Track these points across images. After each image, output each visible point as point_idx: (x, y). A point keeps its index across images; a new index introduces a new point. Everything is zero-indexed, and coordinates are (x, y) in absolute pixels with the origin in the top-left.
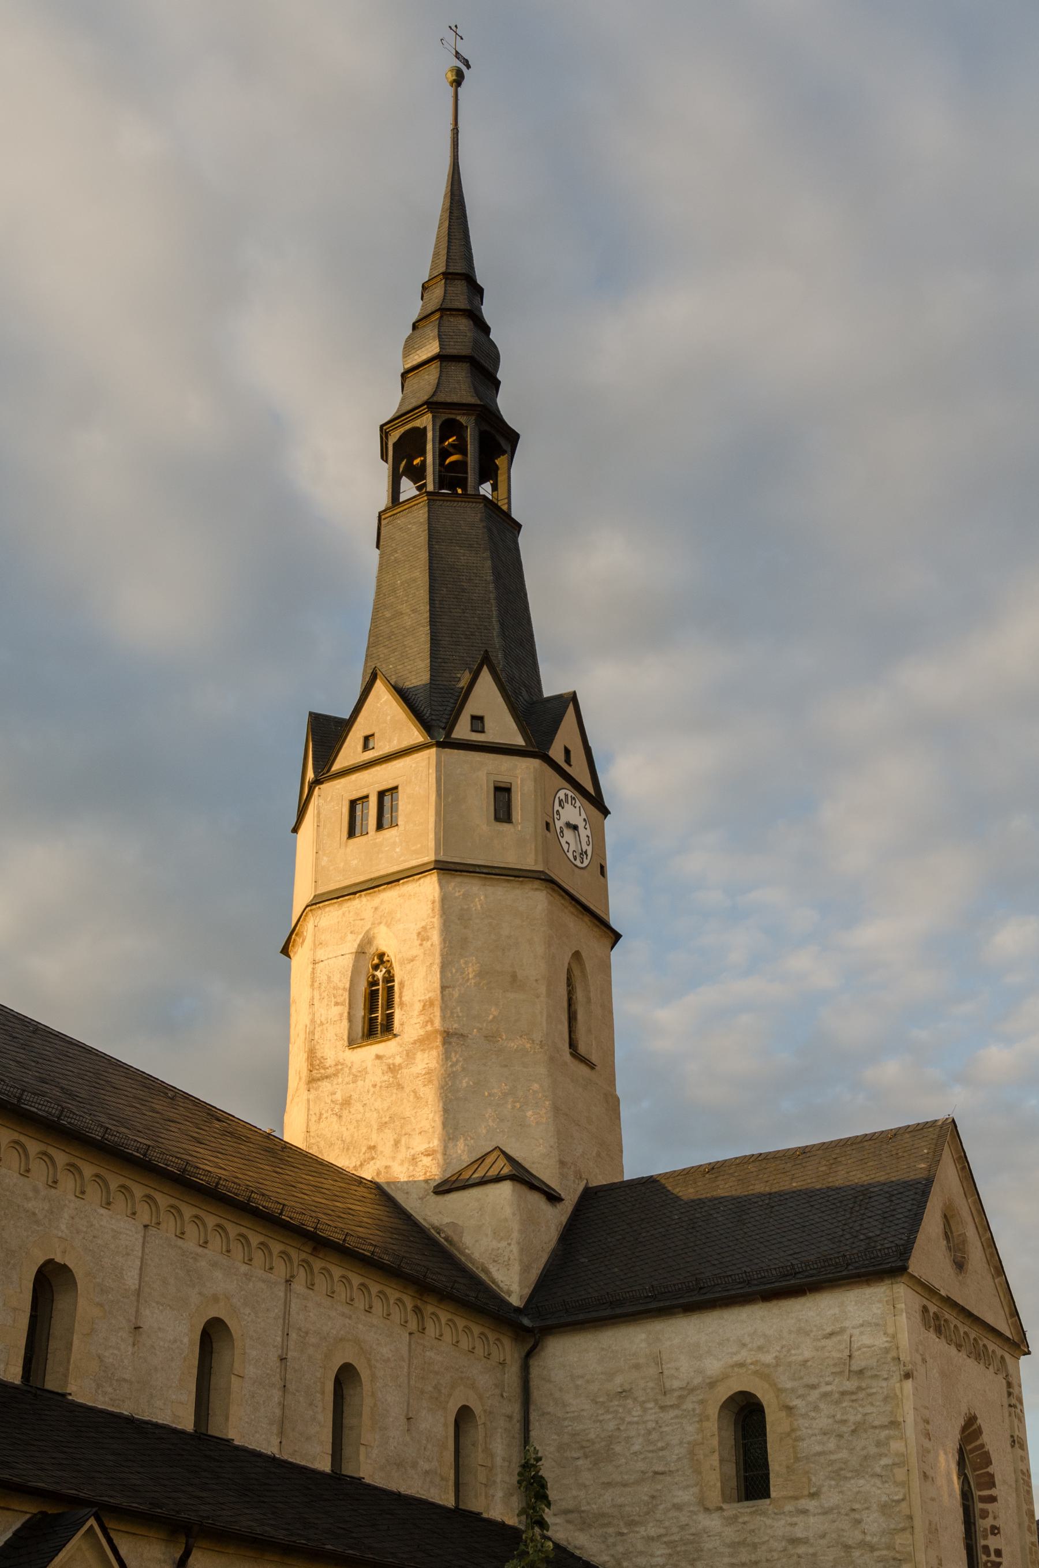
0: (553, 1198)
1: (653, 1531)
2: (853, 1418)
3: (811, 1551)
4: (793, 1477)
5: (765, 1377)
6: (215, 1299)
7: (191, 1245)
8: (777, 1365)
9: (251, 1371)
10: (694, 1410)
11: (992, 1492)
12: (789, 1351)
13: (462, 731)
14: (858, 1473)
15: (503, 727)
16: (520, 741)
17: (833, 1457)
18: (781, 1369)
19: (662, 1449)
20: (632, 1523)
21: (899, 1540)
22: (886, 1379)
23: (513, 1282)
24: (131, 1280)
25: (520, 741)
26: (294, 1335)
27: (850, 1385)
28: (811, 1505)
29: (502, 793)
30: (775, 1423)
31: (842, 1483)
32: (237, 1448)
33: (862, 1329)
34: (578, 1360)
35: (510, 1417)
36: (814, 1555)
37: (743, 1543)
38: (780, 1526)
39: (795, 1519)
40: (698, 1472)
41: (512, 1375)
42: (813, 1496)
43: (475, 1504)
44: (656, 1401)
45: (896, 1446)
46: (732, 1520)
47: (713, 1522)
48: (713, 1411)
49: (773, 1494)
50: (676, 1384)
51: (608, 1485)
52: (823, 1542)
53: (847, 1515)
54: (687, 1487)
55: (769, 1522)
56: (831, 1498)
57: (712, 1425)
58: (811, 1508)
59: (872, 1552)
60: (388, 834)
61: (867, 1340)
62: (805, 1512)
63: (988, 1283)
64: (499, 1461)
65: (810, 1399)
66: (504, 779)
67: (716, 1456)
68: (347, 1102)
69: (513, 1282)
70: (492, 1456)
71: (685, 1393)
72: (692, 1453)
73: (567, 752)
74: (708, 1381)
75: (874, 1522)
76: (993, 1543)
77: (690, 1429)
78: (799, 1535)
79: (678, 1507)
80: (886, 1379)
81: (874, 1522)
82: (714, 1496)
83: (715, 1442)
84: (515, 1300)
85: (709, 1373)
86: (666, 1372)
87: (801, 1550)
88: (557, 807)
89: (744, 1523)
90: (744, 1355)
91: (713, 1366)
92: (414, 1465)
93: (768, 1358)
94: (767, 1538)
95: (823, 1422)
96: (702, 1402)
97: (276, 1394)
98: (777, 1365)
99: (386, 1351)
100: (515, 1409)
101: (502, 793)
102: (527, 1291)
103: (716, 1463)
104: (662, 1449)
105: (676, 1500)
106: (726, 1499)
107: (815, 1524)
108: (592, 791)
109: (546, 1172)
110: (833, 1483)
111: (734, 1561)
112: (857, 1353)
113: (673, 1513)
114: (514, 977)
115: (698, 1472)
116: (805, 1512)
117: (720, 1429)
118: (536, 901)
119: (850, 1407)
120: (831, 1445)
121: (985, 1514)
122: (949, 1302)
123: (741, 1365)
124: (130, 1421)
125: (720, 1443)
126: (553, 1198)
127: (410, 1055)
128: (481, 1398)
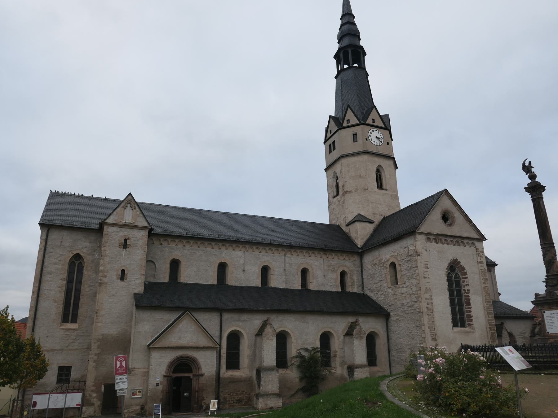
0: (372, 222)
1: (381, 293)
2: (410, 266)
5: (396, 258)
6: (265, 262)
7: (258, 253)
9: (276, 273)
11: (466, 276)
13: (345, 124)
14: (412, 278)
15: (354, 120)
16: (358, 122)
20: (378, 291)
21: (419, 292)
23: (360, 243)
24: (242, 262)
25: (358, 122)
26: (288, 265)
28: (404, 285)
29: (355, 135)
30: (398, 268)
32: (274, 288)
34: (368, 259)
35: (358, 271)
37: (394, 294)
38: (399, 291)
41: (358, 262)
42: (405, 283)
43: (349, 289)
45: (417, 271)
46: (392, 290)
47: (390, 290)
48: (388, 266)
50: (383, 261)
51: (374, 283)
56: (407, 284)
57: (388, 269)
60: (335, 151)
61: (411, 248)
62: (403, 287)
63: (467, 225)
64: (355, 280)
66: (354, 132)
68: (333, 209)
69: (360, 243)
70: (353, 280)
73: (373, 120)
75: (414, 289)
76: (466, 288)
79: (384, 287)
81: (414, 289)
82: (390, 286)
84: (359, 246)
87: (404, 295)
88: (369, 134)
90: (393, 254)
91: (388, 257)
92: (327, 284)
93: (396, 254)
95: (405, 267)
97: (284, 277)
99: (316, 264)
100: (360, 269)
101: (355, 135)
102: (362, 244)
106: (392, 285)
107: (404, 290)
108: (383, 126)
109: (371, 218)
114: (360, 176)
116: (403, 287)
118: (365, 157)
120: (407, 272)
121: (464, 282)
122: (438, 235)
123: (392, 256)
124: (241, 288)
126: (372, 222)
127: (341, 198)
128: (348, 268)
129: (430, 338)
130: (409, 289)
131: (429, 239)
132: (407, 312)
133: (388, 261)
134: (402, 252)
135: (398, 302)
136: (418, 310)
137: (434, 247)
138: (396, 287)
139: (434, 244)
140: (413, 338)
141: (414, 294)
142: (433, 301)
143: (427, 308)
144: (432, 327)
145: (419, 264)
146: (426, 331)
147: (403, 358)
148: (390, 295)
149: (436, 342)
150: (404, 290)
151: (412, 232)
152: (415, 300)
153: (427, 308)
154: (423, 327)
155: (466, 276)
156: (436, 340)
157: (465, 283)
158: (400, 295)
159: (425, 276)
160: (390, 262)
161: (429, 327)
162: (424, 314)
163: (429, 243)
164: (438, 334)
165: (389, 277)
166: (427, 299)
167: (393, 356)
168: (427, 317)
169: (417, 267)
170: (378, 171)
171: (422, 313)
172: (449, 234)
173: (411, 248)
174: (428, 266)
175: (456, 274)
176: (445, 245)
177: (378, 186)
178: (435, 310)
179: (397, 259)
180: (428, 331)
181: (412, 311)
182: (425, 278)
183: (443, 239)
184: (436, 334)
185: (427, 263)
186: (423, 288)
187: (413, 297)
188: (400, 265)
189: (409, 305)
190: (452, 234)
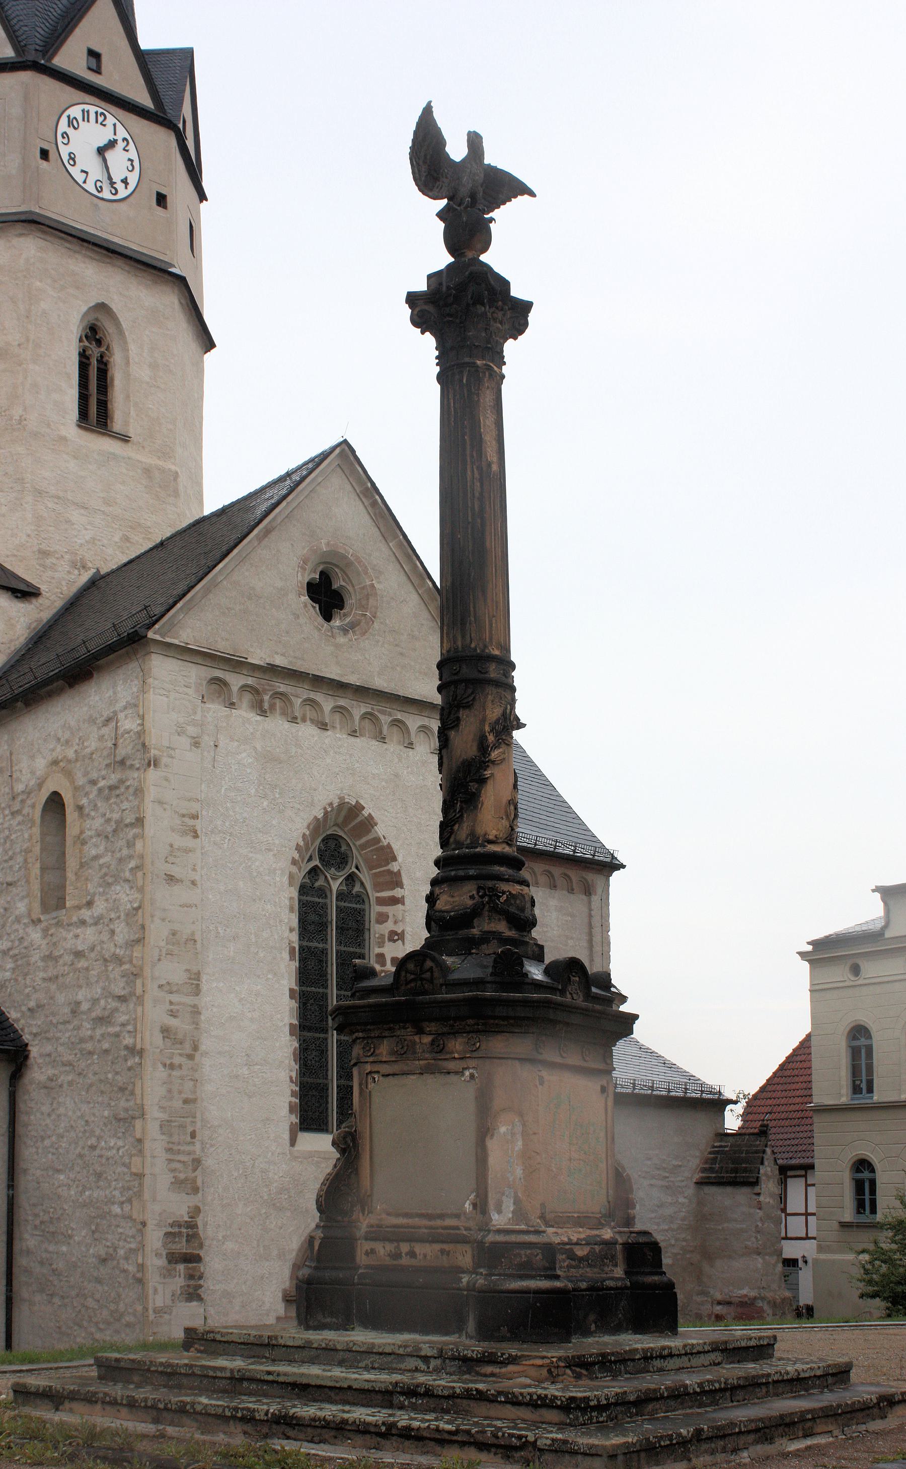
3: (86, 964)
4: (79, 885)
5: (69, 774)
8: (77, 760)
10: (28, 814)
12: (83, 743)
17: (102, 861)
18: (78, 764)
19: (11, 858)
22: (138, 769)
27: (114, 778)
28: (86, 914)
31: (107, 890)
33: (126, 712)
36: (87, 969)
39: (79, 931)
40: (28, 882)
44: (9, 806)
49: (68, 904)
50: (20, 787)
52: (93, 955)
53: (107, 925)
54: (23, 898)
55: (64, 933)
56: (100, 907)
57: (36, 830)
58: (87, 919)
59: (121, 965)
62: (83, 923)
65: (91, 797)
67: (38, 865)
71: (24, 797)
72: (26, 860)
74: (38, 781)
77: (26, 836)
78: (80, 948)
80: (138, 769)
81: (123, 932)
83: (37, 849)
85: (38, 773)
86: (14, 776)
87: (83, 963)
89: (52, 935)
94: (62, 952)
96: (33, 806)
98: (77, 760)
103: (38, 872)
104: (11, 858)
105: (17, 912)
110: (101, 890)
111: (45, 975)
112: (121, 741)
113: (16, 926)
115: (28, 882)
116: (83, 923)
117: (43, 835)
119: (115, 803)
125: (43, 850)
129: (164, 1180)
130: (105, 937)
131: (219, 683)
132: (89, 1046)
133: (40, 786)
134: (92, 744)
135: (61, 998)
136: (128, 1041)
137: (247, 734)
138: (59, 924)
139: (244, 714)
140: (99, 1176)
141: (119, 960)
142: (204, 1000)
143: (166, 1031)
144: (185, 1125)
145: (150, 810)
146: (147, 1145)
147: (60, 1265)
148: (35, 957)
149: (193, 1200)
150: (89, 935)
151: (131, 643)
152: (119, 988)
153: (166, 1031)
154: (138, 1124)
155: (397, 893)
156: (196, 1190)
157: (389, 926)
158: (68, 958)
159: (175, 871)
160: (44, 795)
161: (165, 1126)
162: (148, 1062)
163: (216, 710)
164: (209, 1162)
165: (36, 870)
166: (168, 988)
167: (29, 1252)
168: (161, 1073)
169: (140, 821)
170: (93, 334)
171: (141, 1053)
172: (332, 672)
173: (129, 724)
174: (198, 824)
175: (351, 879)
176: (307, 731)
177: (83, 414)
178: (206, 1044)
179: (72, 782)
180: (156, 1143)
181: (106, 1046)
182: (171, 879)
183: (300, 694)
184: (197, 1163)
185: (195, 807)
186: (157, 933)
187: (115, 972)
188: (80, 808)
189: (97, 1012)
190: (353, 679)
